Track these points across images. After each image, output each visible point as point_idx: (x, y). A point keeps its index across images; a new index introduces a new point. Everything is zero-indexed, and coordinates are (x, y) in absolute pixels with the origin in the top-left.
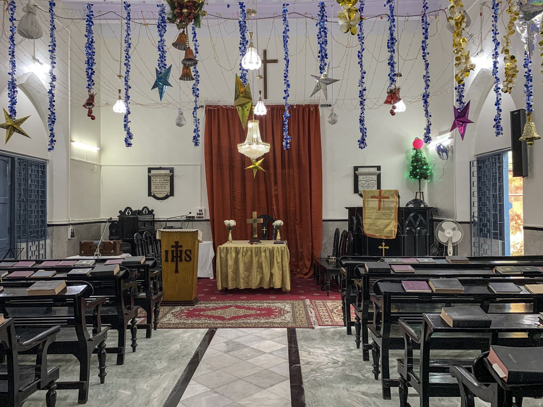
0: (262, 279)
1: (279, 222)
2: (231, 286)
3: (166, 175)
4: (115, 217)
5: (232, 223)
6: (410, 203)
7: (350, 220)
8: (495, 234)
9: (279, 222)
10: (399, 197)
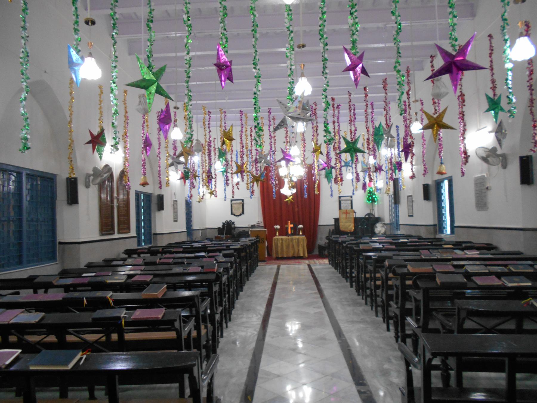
0: (294, 253)
1: (301, 226)
2: (280, 256)
3: (240, 203)
4: (220, 225)
5: (278, 227)
6: (366, 215)
7: (335, 225)
8: (397, 228)
9: (301, 226)
10: (355, 213)
